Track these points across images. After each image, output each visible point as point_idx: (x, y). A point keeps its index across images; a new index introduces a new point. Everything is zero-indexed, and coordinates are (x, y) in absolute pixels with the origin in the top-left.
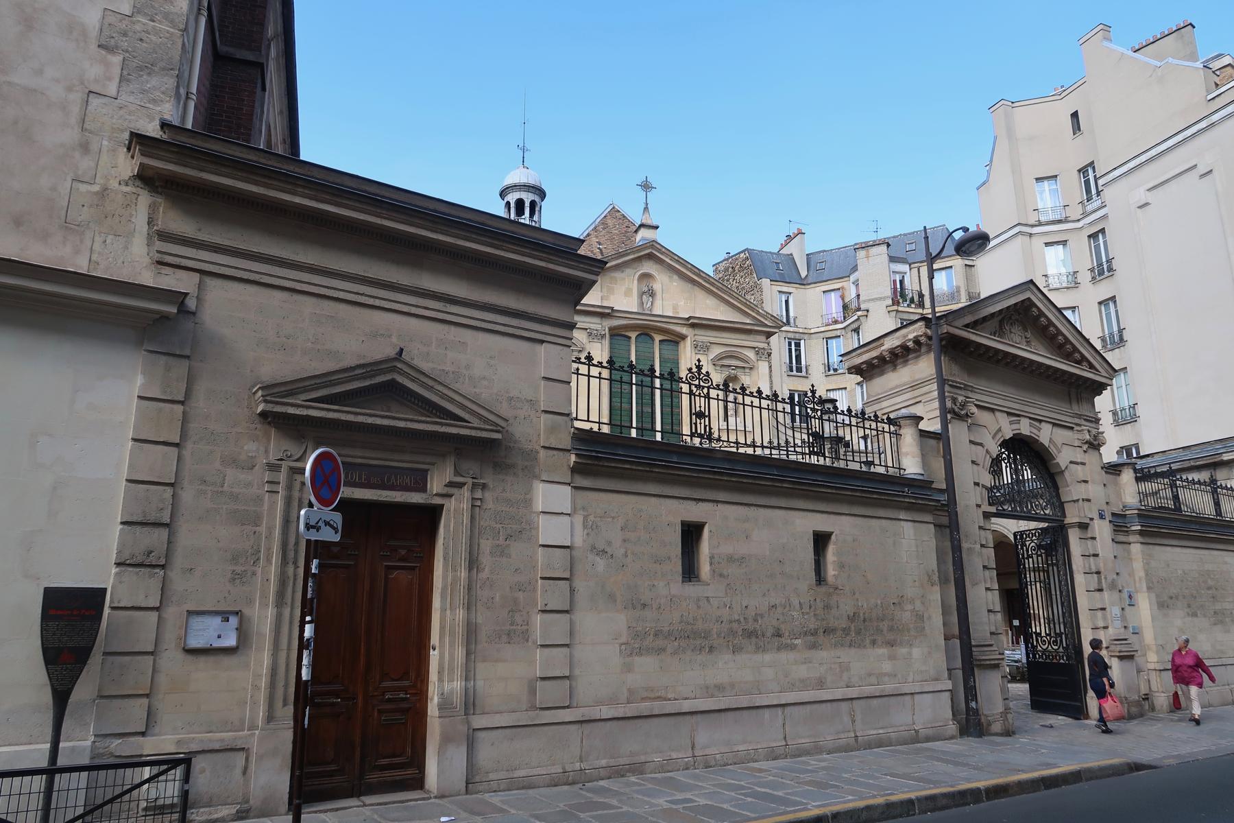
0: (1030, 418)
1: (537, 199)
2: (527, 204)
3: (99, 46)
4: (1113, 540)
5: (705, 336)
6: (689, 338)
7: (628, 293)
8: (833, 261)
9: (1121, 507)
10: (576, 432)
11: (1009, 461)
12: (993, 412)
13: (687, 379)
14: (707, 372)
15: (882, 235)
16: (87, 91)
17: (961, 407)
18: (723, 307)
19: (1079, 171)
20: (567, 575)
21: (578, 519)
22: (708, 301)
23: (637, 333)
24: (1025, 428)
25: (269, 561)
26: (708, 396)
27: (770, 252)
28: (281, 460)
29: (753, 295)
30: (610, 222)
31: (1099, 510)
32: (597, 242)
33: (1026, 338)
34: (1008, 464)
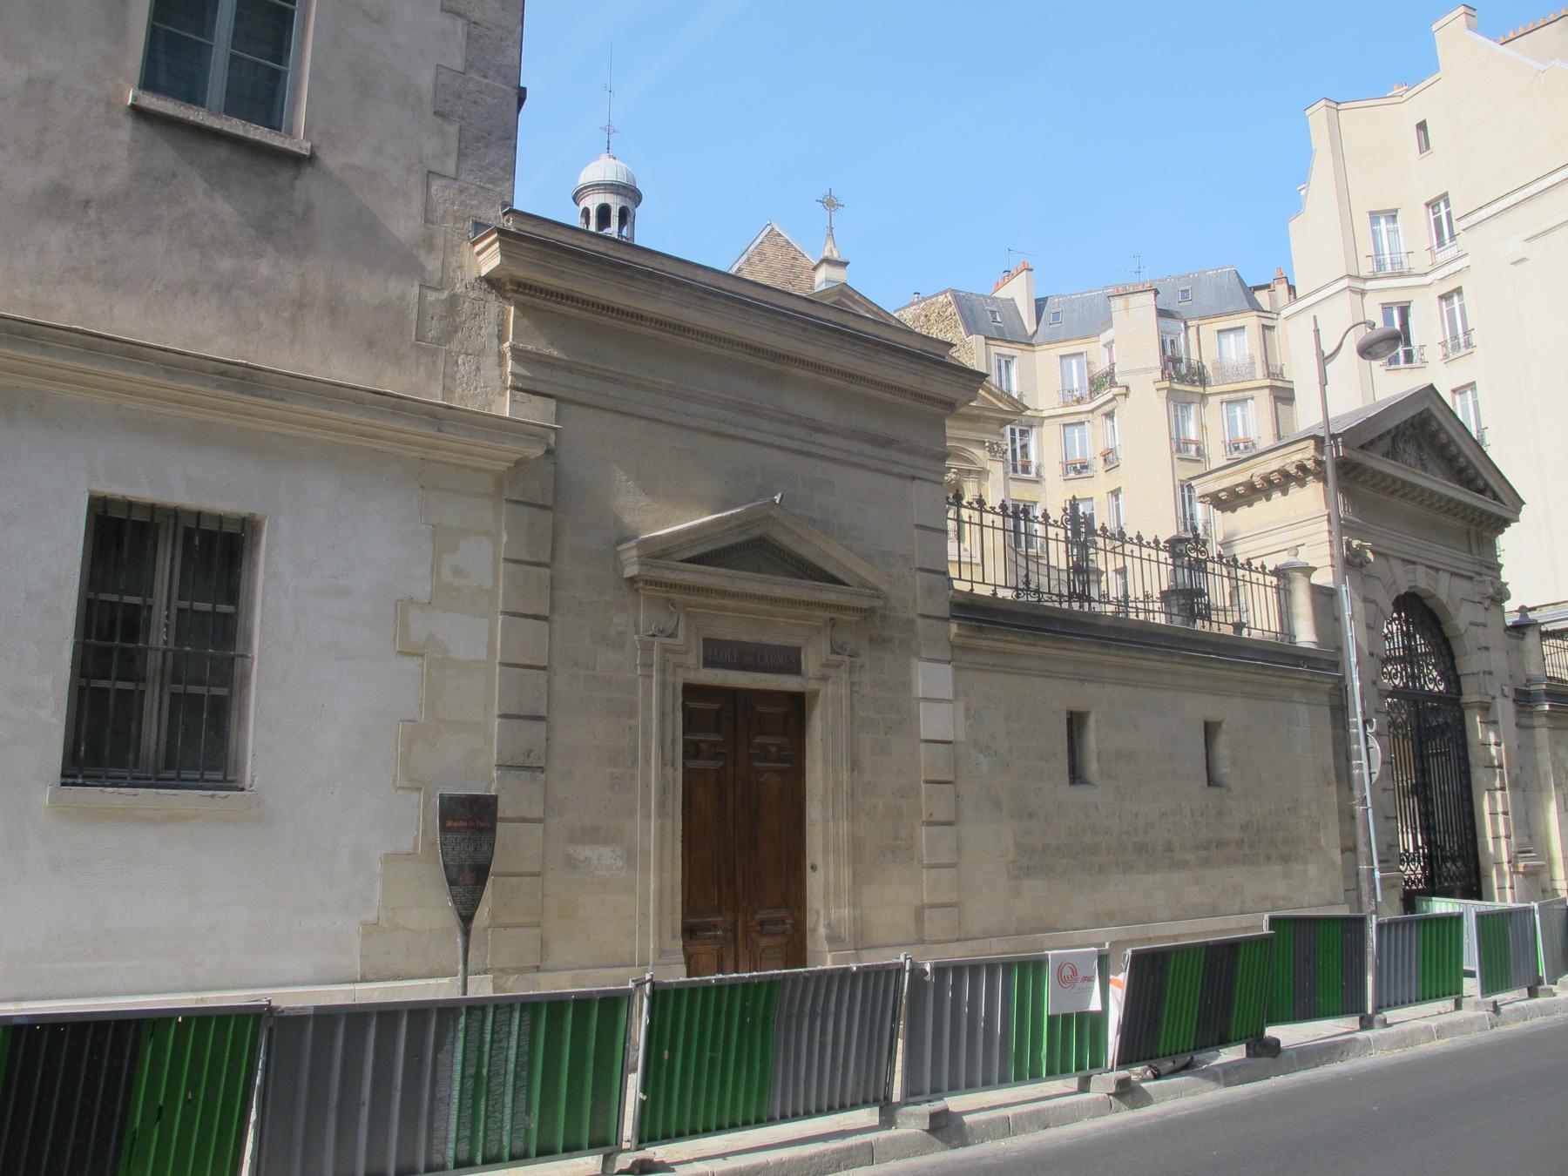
0: (1427, 566)
1: (629, 205)
2: (615, 213)
3: (435, 113)
4: (1517, 725)
9: (1525, 681)
10: (956, 595)
13: (1062, 523)
15: (1147, 277)
16: (426, 170)
19: (1428, 205)
20: (950, 778)
21: (961, 705)
24: (1421, 580)
25: (647, 761)
28: (654, 636)
31: (1502, 685)
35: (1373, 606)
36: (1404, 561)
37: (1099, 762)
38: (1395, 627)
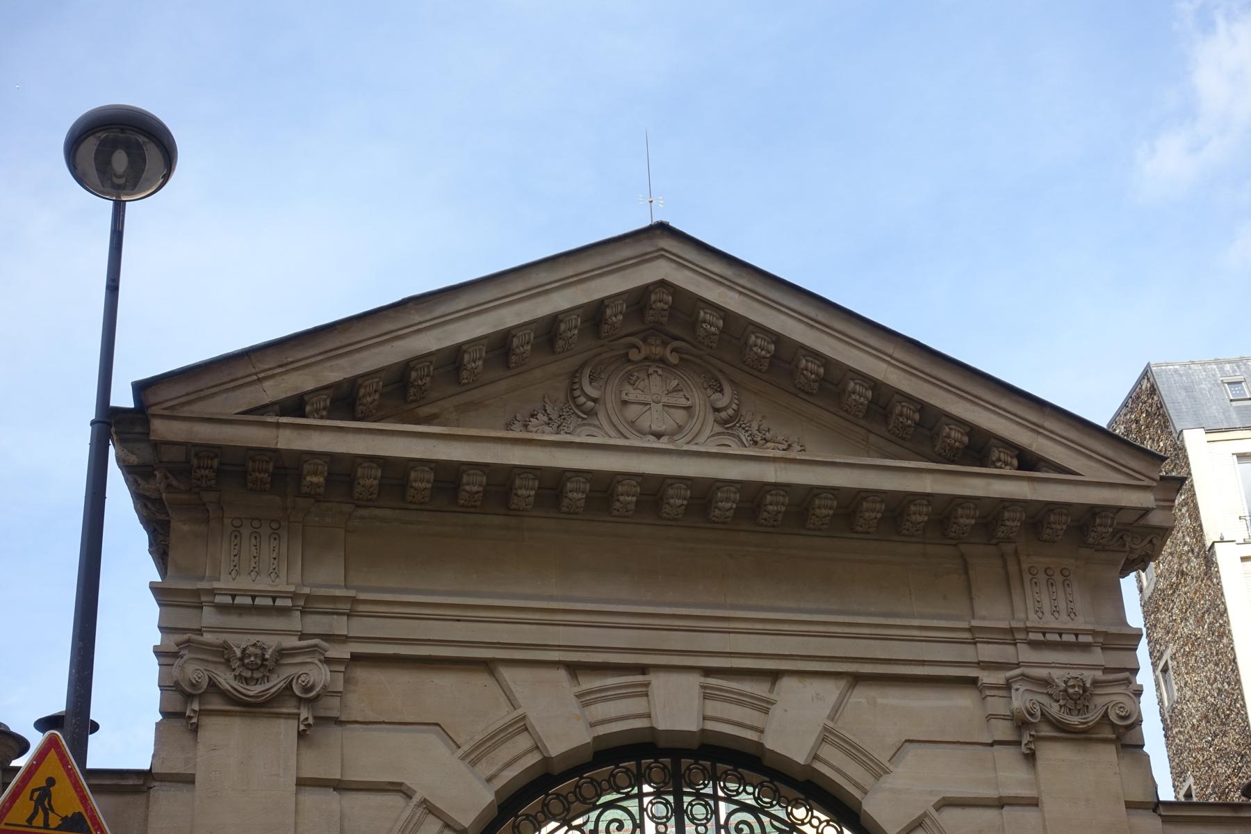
0: (708, 672)
12: (492, 673)
17: (248, 674)
35: (396, 800)
36: (575, 669)
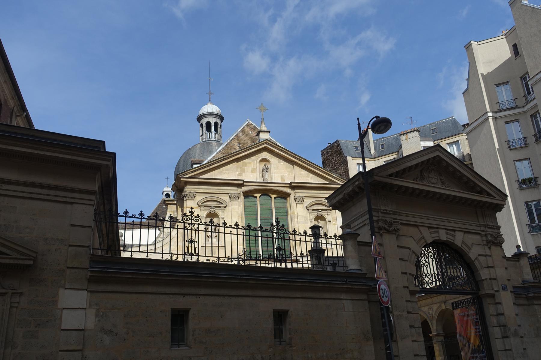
0: (446, 229)
1: (218, 121)
2: (213, 125)
4: (514, 304)
5: (300, 193)
6: (292, 195)
7: (254, 171)
8: (389, 143)
11: (434, 257)
12: (418, 228)
14: (198, 215)
15: (416, 127)
17: (389, 226)
18: (311, 175)
19: (521, 78)
21: (92, 312)
22: (302, 172)
23: (260, 195)
24: (443, 236)
26: (198, 230)
27: (352, 141)
29: (343, 166)
30: (246, 131)
31: (502, 285)
32: (238, 143)
33: (441, 180)
34: (434, 259)
35: (408, 250)
37: (193, 335)
38: (430, 260)
